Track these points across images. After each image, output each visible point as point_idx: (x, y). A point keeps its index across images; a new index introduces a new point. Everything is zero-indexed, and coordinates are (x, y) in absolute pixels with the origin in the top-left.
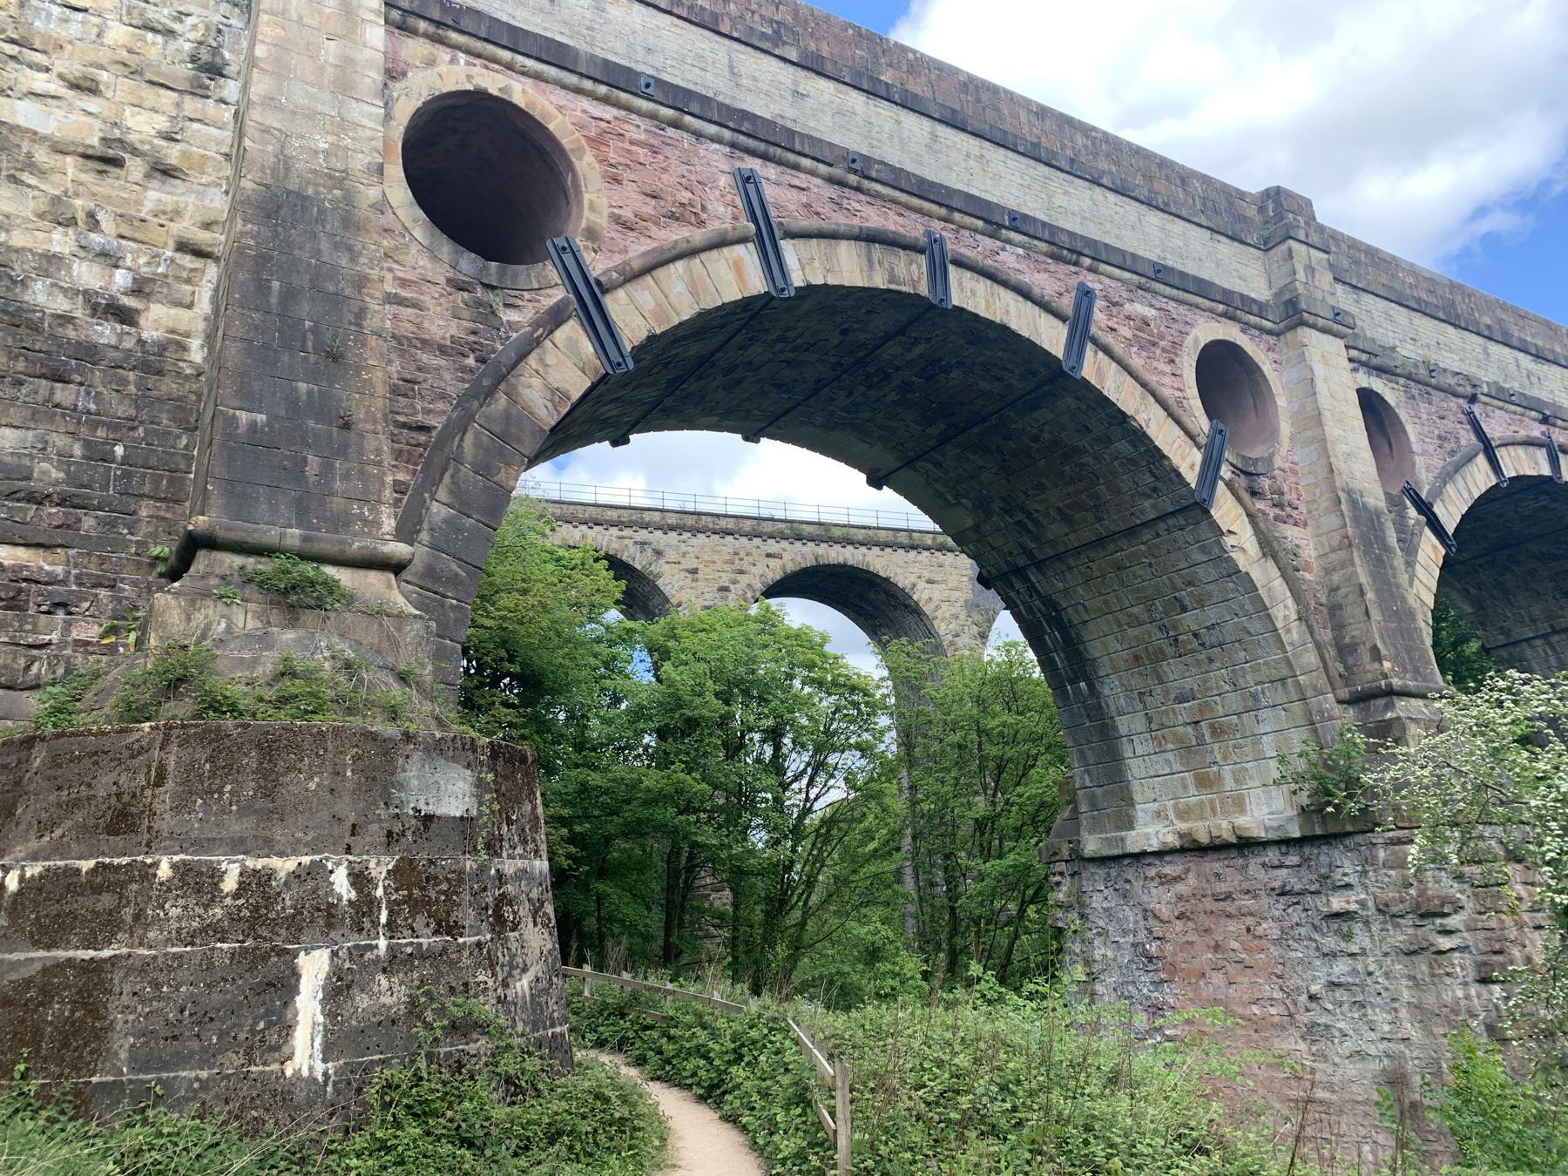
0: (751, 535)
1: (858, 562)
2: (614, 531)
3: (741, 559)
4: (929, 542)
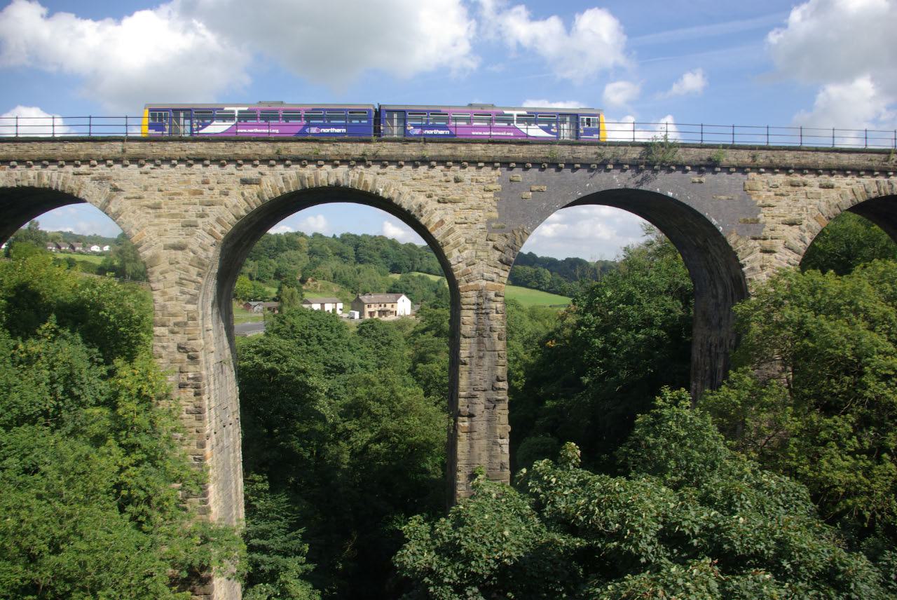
2: (70, 169)
4: (448, 152)
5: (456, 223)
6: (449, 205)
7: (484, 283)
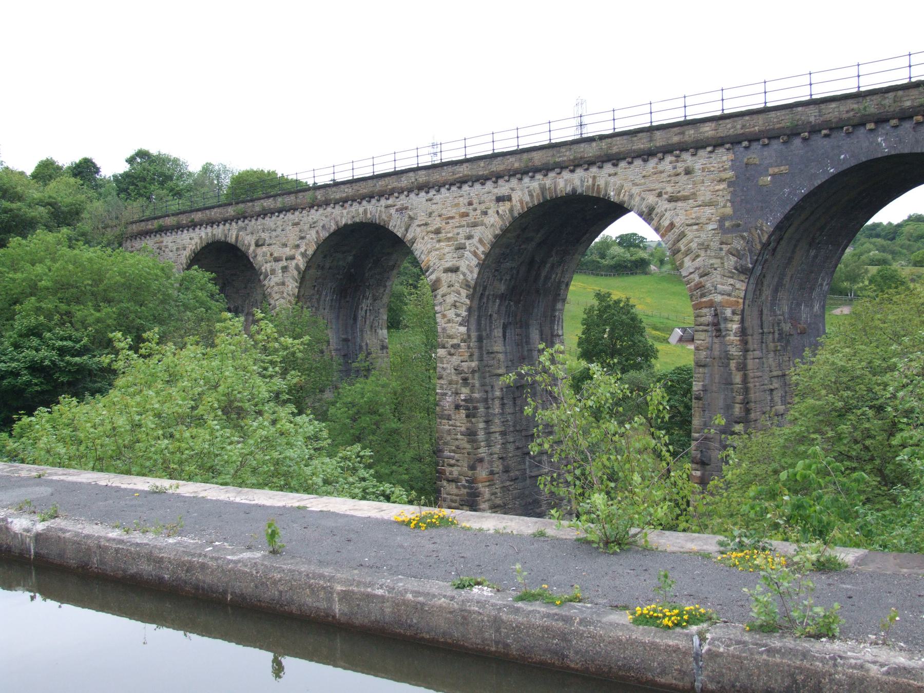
0: (482, 180)
1: (588, 187)
3: (475, 210)
4: (676, 139)
5: (688, 225)
6: (680, 204)
7: (718, 298)
